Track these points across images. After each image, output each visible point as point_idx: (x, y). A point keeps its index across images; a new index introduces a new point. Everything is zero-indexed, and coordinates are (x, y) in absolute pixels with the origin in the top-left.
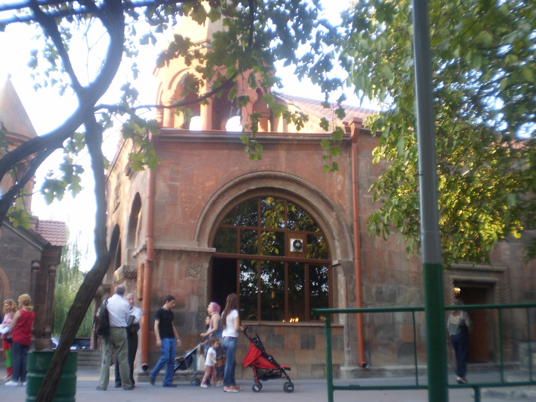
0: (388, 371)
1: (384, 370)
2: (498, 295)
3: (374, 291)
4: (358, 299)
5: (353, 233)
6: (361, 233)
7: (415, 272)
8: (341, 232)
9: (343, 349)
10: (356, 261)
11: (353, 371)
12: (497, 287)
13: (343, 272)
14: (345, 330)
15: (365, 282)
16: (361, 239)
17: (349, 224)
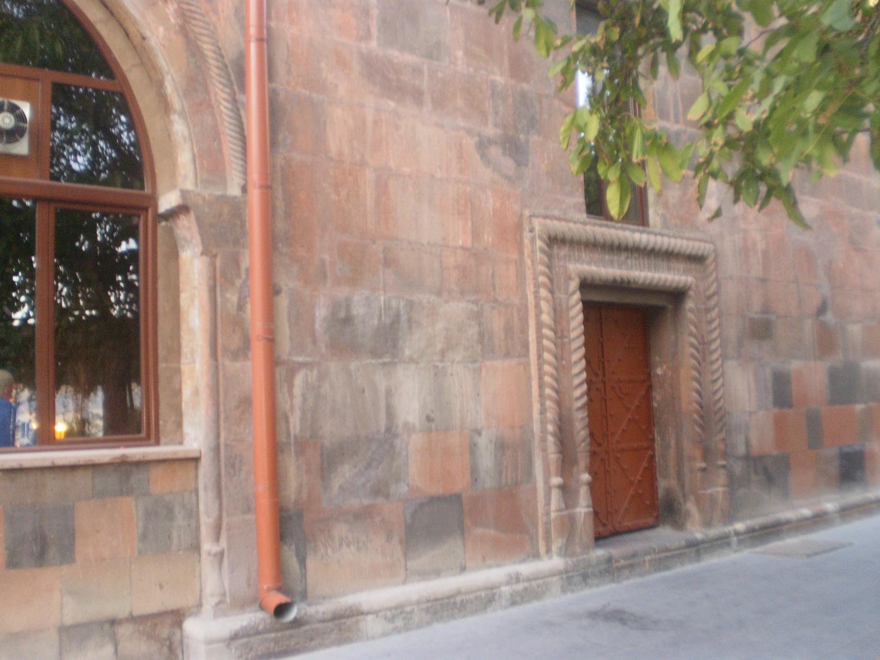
0: (368, 613)
1: (356, 613)
2: (692, 328)
3: (321, 312)
4: (258, 349)
5: (243, 86)
6: (274, 93)
7: (462, 248)
8: (195, 83)
9: (196, 547)
10: (255, 195)
11: (235, 637)
12: (689, 304)
13: (197, 239)
14: (205, 468)
15: (287, 282)
16: (274, 113)
17: (230, 53)
